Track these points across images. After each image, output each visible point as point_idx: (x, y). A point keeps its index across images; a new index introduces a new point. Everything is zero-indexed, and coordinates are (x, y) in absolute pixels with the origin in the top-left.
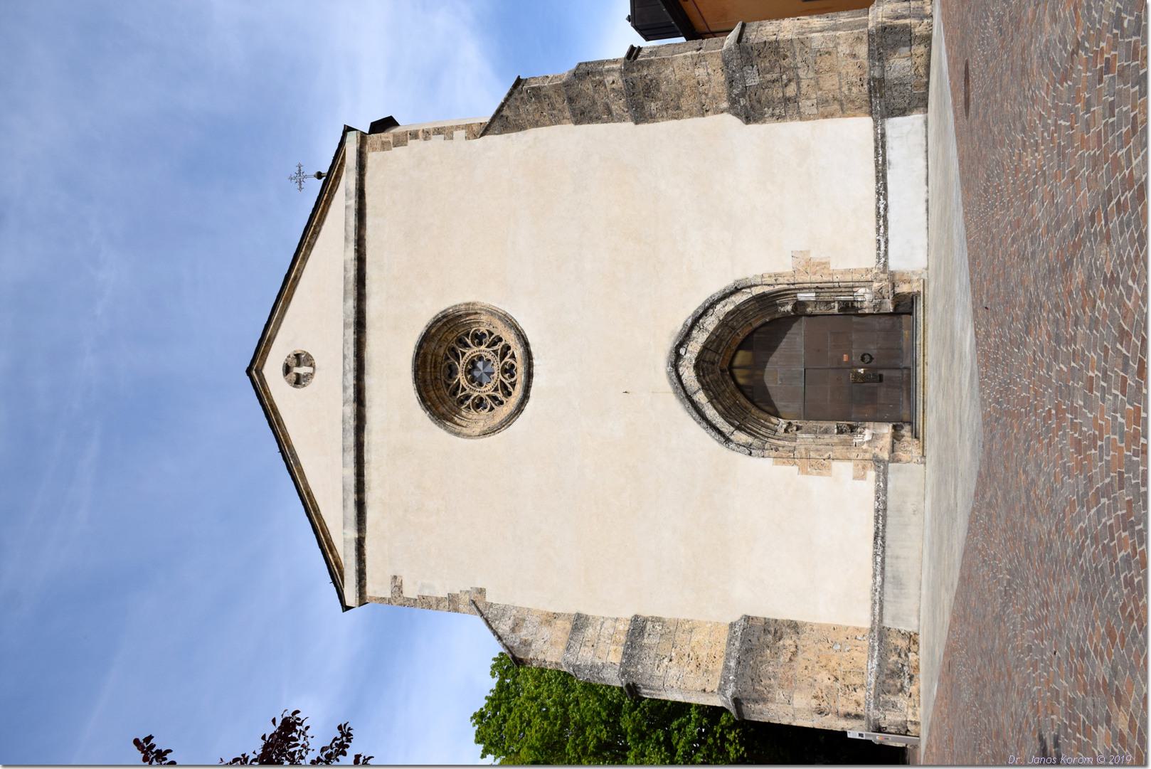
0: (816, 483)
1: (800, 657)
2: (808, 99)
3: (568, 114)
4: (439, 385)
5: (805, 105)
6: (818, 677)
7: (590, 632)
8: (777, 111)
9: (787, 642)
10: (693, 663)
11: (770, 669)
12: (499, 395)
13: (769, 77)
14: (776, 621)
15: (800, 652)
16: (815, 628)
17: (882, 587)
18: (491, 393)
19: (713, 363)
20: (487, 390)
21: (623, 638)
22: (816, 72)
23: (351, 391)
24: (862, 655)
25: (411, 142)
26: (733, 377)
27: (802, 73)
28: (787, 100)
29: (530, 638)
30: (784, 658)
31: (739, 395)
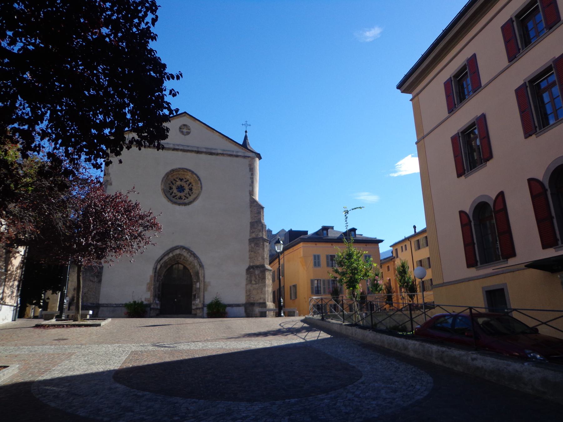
0: (144, 287)
1: (92, 283)
2: (251, 287)
3: (253, 221)
4: (177, 175)
5: (249, 286)
8: (248, 278)
9: (96, 279)
11: (88, 274)
12: (173, 194)
13: (257, 277)
17: (113, 306)
18: (174, 192)
19: (180, 259)
20: (175, 191)
22: (257, 289)
23: (177, 147)
25: (250, 173)
26: (176, 264)
27: (257, 285)
28: (251, 281)
30: (91, 278)
31: (170, 265)
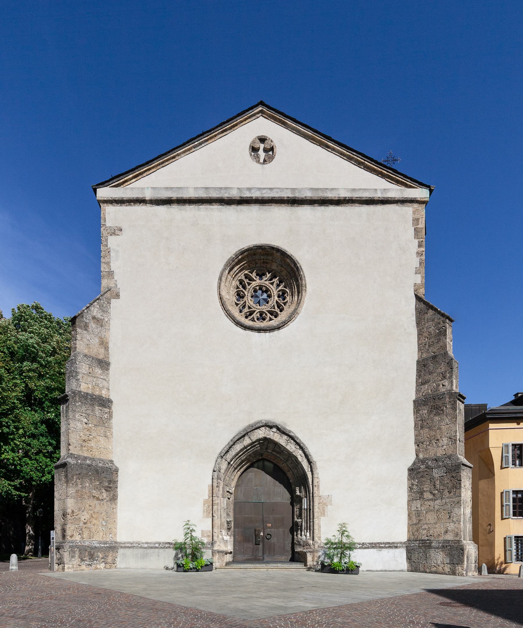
1: (97, 502)
6: (85, 513)
7: (98, 371)
9: (105, 494)
10: (86, 438)
14: (117, 488)
15: (99, 502)
16: (114, 510)
21: (97, 393)
24: (101, 537)
29: (90, 330)
30: (95, 493)
